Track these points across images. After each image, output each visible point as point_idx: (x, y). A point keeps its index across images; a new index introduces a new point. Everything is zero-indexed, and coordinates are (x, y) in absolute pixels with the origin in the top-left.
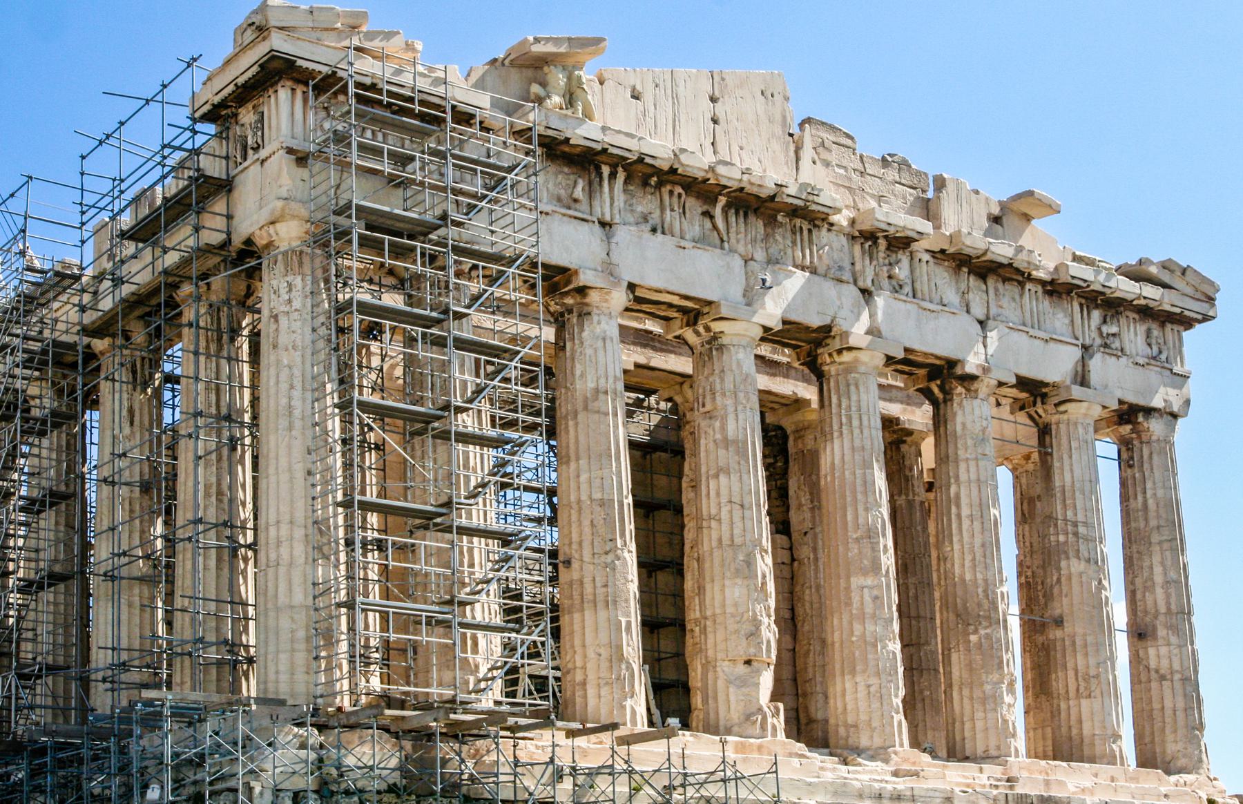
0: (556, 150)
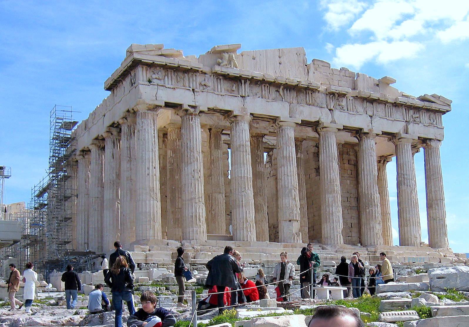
0: (227, 77)
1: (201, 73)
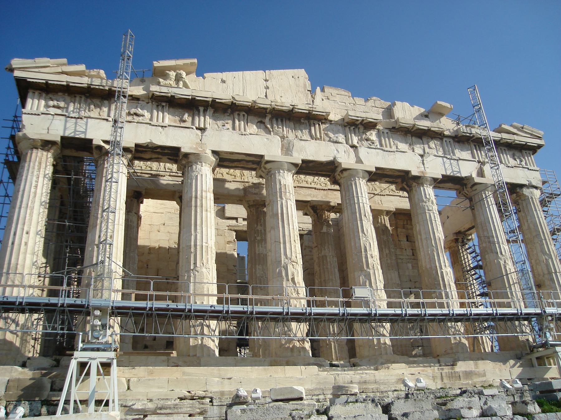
1: (130, 98)
